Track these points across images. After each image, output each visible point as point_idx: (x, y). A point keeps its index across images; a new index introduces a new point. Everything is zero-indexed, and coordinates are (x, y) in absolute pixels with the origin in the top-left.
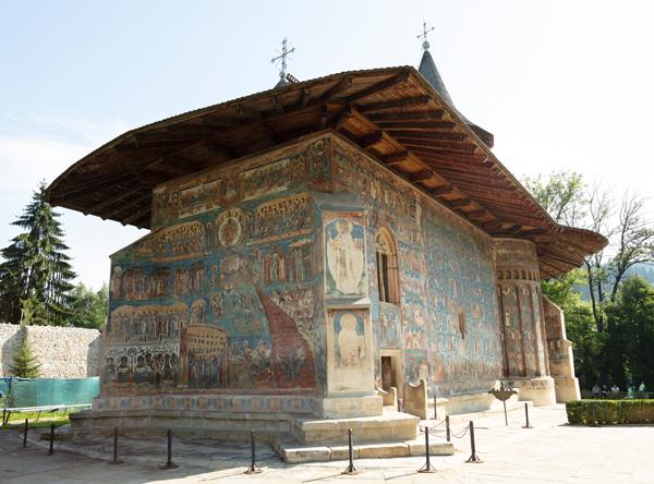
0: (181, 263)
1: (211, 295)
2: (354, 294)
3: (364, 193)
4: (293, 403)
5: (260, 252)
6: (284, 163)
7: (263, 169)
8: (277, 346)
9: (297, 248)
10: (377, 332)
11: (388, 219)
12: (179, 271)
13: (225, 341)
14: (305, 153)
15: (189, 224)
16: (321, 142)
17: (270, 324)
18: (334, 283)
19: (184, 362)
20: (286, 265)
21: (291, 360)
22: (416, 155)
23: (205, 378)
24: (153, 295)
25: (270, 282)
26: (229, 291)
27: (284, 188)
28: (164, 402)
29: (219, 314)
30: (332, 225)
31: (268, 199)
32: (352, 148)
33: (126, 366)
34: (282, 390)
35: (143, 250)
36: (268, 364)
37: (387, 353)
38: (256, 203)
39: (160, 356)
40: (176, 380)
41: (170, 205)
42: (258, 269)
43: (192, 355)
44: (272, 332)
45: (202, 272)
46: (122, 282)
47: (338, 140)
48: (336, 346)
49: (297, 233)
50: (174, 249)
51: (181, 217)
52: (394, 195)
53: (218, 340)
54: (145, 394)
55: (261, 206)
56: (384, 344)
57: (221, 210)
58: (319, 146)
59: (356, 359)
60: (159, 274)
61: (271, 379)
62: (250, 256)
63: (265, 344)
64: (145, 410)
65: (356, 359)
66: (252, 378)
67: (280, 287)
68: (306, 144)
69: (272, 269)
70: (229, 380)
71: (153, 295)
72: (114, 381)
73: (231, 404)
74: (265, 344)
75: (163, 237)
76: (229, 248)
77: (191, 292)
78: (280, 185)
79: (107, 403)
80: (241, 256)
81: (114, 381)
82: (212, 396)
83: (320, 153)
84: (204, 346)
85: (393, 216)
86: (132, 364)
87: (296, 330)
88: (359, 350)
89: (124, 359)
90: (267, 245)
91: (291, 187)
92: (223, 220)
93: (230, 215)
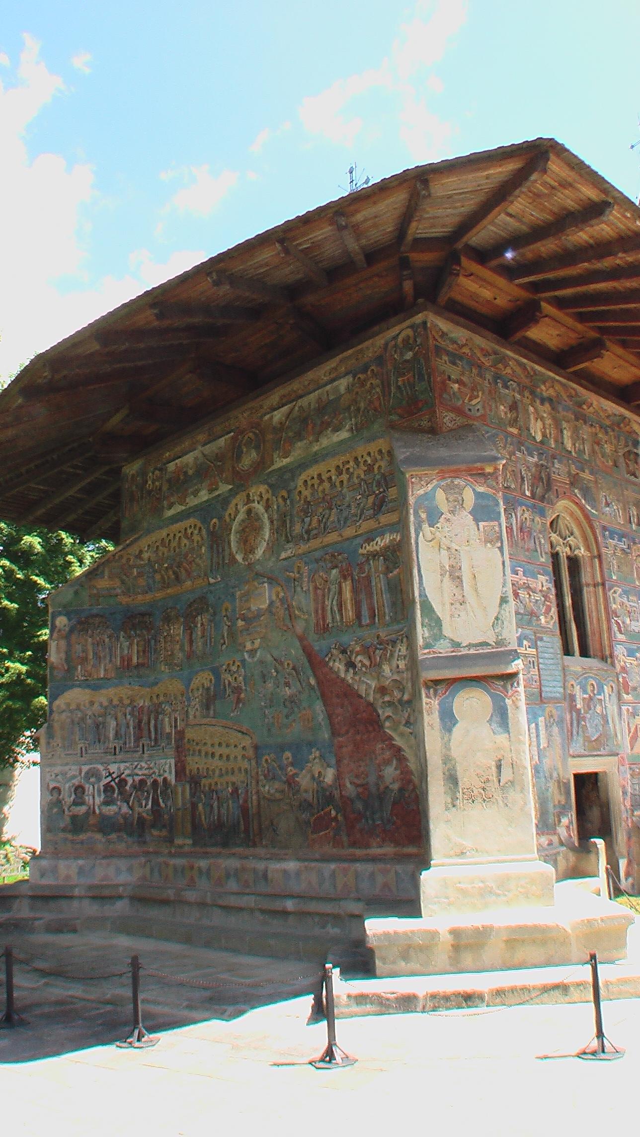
1: (224, 660)
2: (485, 644)
3: (514, 431)
4: (380, 879)
5: (305, 570)
6: (343, 384)
7: (303, 402)
9: (374, 555)
10: (561, 721)
11: (575, 481)
12: (168, 620)
13: (250, 753)
14: (380, 360)
16: (409, 332)
17: (330, 716)
18: (438, 622)
19: (183, 793)
20: (355, 591)
21: (373, 790)
22: (624, 344)
23: (219, 826)
24: (126, 666)
26: (252, 652)
27: (344, 435)
29: (239, 700)
30: (429, 497)
31: (315, 459)
32: (479, 341)
33: (83, 803)
35: (103, 583)
36: (329, 799)
37: (588, 766)
38: (293, 471)
39: (142, 782)
41: (149, 492)
43: (195, 781)
44: (334, 733)
46: (69, 645)
47: (443, 325)
48: (447, 759)
49: (372, 524)
50: (158, 577)
51: (170, 513)
52: (586, 431)
53: (238, 752)
54: (120, 856)
55: (303, 477)
56: (577, 746)
57: (233, 493)
58: (406, 341)
59: (493, 786)
60: (134, 627)
62: (288, 579)
63: (322, 757)
64: (118, 886)
65: (493, 786)
67: (345, 639)
68: (379, 341)
70: (260, 829)
71: (126, 666)
72: (64, 830)
73: (265, 876)
75: (139, 556)
76: (250, 566)
77: (189, 657)
78: (337, 429)
79: (54, 870)
80: (272, 580)
81: (64, 830)
82: (233, 863)
83: (409, 355)
84: (216, 763)
85: (586, 476)
86: (95, 798)
87: (381, 727)
88: (499, 767)
89: (79, 790)
90: (317, 554)
91: (357, 430)
92: (237, 512)
93: (249, 500)
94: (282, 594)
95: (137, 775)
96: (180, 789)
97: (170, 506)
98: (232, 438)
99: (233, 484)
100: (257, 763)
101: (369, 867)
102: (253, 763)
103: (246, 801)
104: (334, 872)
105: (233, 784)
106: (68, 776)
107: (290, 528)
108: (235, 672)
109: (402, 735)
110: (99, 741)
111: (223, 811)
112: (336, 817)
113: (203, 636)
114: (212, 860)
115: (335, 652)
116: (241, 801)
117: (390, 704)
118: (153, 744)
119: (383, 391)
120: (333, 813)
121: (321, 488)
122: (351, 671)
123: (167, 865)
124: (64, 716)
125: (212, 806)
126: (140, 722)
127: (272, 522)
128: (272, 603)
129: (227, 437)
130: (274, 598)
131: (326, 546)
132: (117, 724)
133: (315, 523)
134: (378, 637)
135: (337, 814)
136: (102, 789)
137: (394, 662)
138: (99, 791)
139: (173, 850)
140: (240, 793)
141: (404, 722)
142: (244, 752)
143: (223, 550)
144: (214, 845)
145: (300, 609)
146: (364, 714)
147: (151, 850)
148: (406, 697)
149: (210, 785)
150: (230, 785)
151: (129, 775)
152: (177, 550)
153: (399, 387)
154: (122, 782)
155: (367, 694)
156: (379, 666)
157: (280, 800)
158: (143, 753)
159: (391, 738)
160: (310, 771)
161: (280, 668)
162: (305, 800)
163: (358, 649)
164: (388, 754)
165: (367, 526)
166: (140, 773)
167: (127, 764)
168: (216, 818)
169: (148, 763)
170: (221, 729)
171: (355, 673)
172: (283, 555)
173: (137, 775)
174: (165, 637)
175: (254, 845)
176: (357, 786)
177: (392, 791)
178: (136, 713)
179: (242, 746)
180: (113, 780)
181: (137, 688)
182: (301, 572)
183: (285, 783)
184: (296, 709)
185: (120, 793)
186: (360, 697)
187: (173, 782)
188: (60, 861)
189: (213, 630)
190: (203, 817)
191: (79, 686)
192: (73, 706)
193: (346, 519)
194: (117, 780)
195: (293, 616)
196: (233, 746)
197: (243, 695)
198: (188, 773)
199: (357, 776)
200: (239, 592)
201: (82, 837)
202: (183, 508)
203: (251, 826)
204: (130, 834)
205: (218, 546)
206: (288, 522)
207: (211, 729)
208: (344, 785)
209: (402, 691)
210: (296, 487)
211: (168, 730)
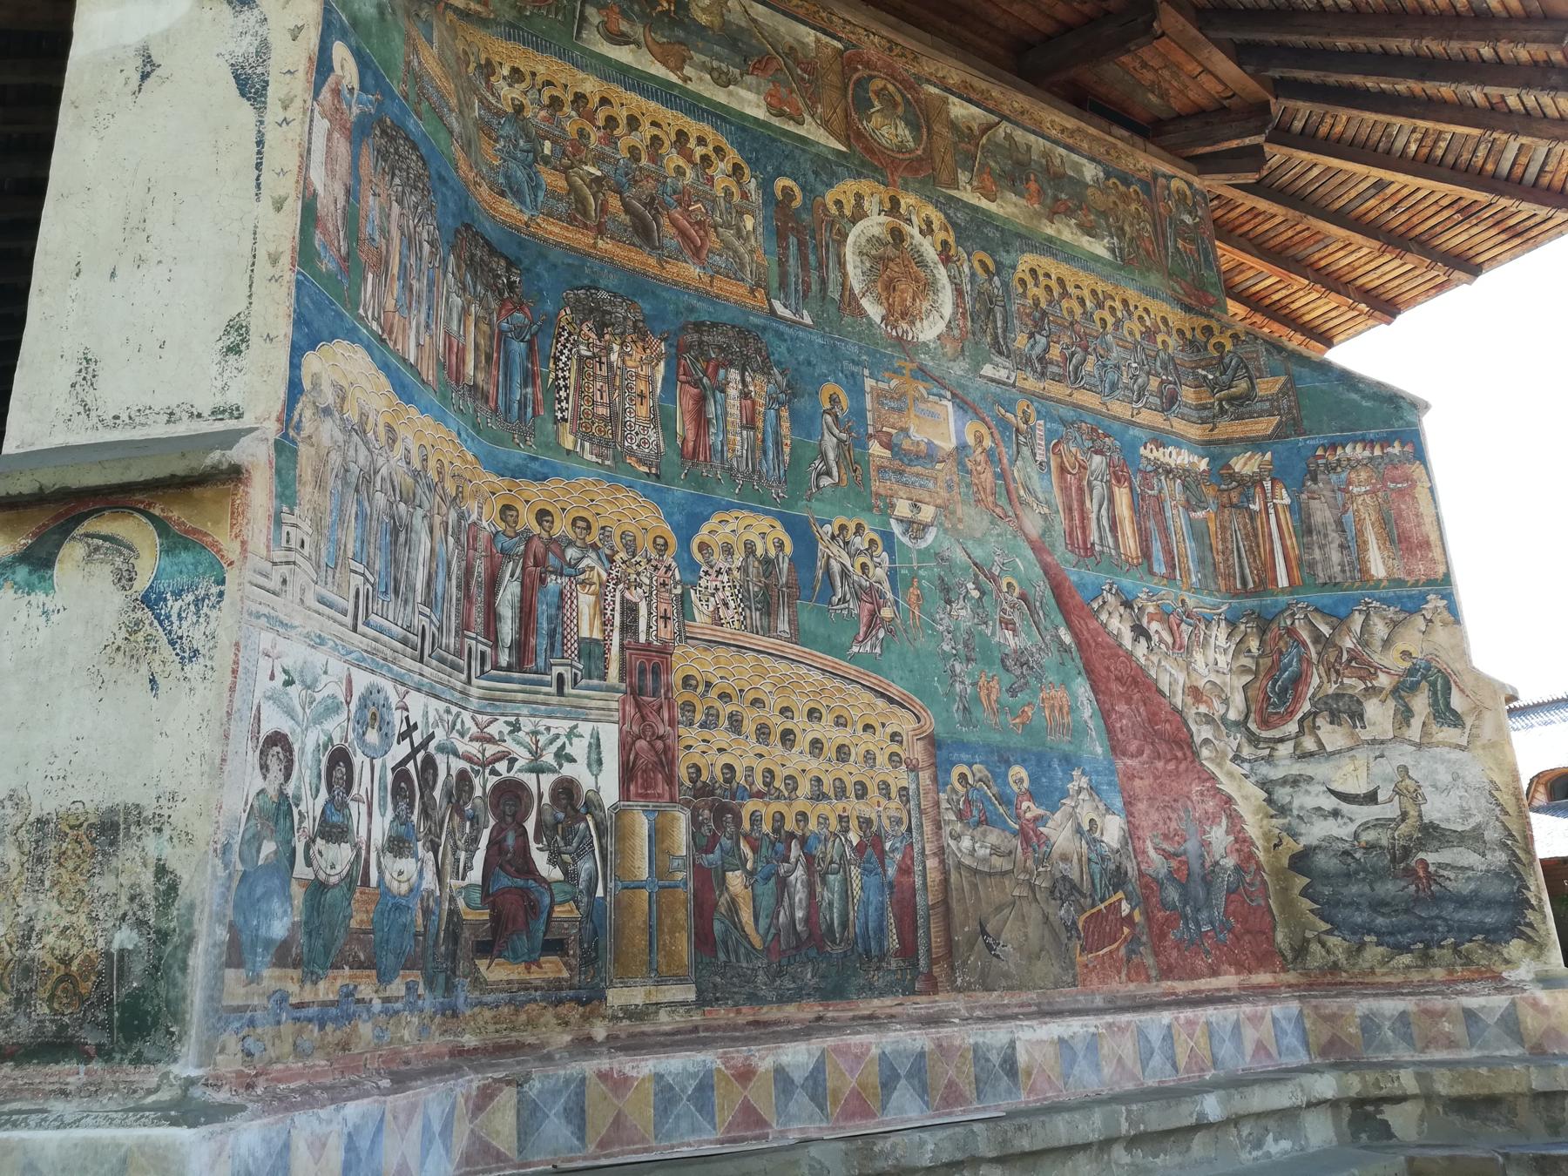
0: (610, 280)
4: (1250, 1035)
7: (1019, 135)
8: (1142, 806)
13: (918, 752)
14: (1147, 186)
15: (674, 120)
17: (1105, 714)
20: (1135, 508)
21: (1196, 867)
25: (1088, 550)
27: (1099, 248)
28: (528, 1117)
29: (874, 620)
31: (1050, 247)
34: (1182, 987)
36: (1118, 879)
40: (590, 958)
42: (1036, 483)
44: (1116, 748)
45: (760, 387)
61: (1134, 940)
62: (1004, 425)
66: (1060, 937)
67: (1126, 582)
69: (1092, 506)
70: (949, 944)
73: (1010, 1065)
74: (1093, 789)
78: (1089, 231)
81: (283, 955)
84: (797, 760)
87: (1196, 754)
92: (859, 215)
94: (988, 443)
95: (456, 754)
96: (642, 825)
97: (619, 39)
98: (840, 53)
99: (849, 146)
100: (935, 780)
101: (1230, 1012)
102: (925, 777)
103: (906, 870)
104: (1169, 1027)
105: (865, 823)
106: (319, 697)
107: (1005, 330)
108: (859, 552)
109: (1230, 775)
110: (396, 592)
111: (829, 894)
112: (1130, 916)
113: (750, 425)
114: (831, 1041)
115: (1110, 598)
116: (891, 871)
117: (1209, 719)
118: (504, 659)
119: (1155, 231)
120: (1125, 908)
121: (1065, 304)
122: (1143, 640)
123: (619, 1084)
124: (328, 431)
125: (783, 884)
126: (468, 571)
127: (959, 292)
128: (962, 448)
129: (825, 39)
130: (970, 440)
131: (1082, 407)
132: (432, 550)
133: (1055, 353)
134: (1183, 601)
135: (1133, 909)
136: (390, 777)
137: (1211, 652)
138: (383, 787)
139: (600, 1031)
140: (887, 846)
141: (1231, 756)
142: (895, 748)
143: (821, 265)
144: (798, 996)
145: (1027, 488)
146: (1168, 726)
147: (470, 1040)
148: (1233, 715)
149: (780, 818)
150: (854, 824)
151: (441, 749)
152: (644, 162)
153: (1177, 249)
154: (429, 764)
155: (1173, 693)
156: (1189, 651)
157: (1004, 874)
158: (469, 682)
159: (1213, 778)
160: (1072, 815)
161: (991, 586)
162: (1064, 878)
163: (1151, 609)
164: (1211, 805)
165: (1146, 417)
166: (461, 748)
167: (442, 706)
168: (799, 914)
169: (479, 717)
170: (817, 675)
171: (1150, 649)
172: (988, 370)
173: (456, 754)
174: (581, 358)
175: (932, 987)
176: (1168, 856)
177: (1224, 869)
178: (463, 538)
179: (889, 730)
180: (415, 751)
181: (470, 457)
182: (1031, 423)
183: (1015, 834)
184: (1033, 681)
185: (426, 813)
186: (1164, 696)
187: (610, 793)
188: (301, 1118)
189: (786, 425)
190: (746, 916)
191: (368, 348)
192: (352, 415)
193: (1114, 386)
194: (420, 756)
195: (1014, 496)
196: (860, 727)
197: (886, 613)
198: (682, 772)
199: (1166, 837)
200: (873, 382)
201: (326, 990)
202: (673, 78)
203: (920, 932)
204: (430, 984)
205: (801, 244)
206: (999, 316)
207: (782, 667)
208: (1144, 852)
209: (1226, 701)
210: (1014, 267)
211: (588, 627)
